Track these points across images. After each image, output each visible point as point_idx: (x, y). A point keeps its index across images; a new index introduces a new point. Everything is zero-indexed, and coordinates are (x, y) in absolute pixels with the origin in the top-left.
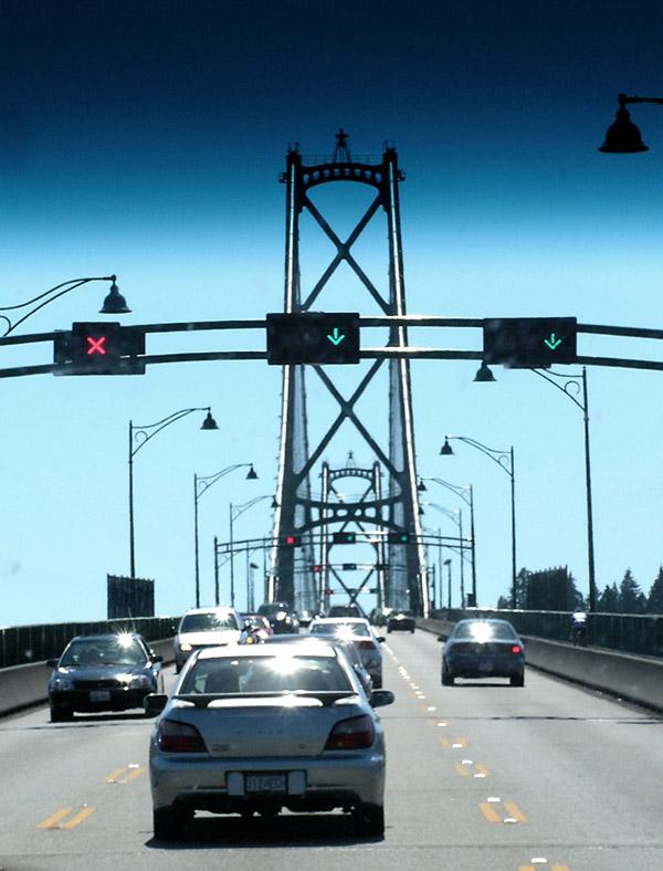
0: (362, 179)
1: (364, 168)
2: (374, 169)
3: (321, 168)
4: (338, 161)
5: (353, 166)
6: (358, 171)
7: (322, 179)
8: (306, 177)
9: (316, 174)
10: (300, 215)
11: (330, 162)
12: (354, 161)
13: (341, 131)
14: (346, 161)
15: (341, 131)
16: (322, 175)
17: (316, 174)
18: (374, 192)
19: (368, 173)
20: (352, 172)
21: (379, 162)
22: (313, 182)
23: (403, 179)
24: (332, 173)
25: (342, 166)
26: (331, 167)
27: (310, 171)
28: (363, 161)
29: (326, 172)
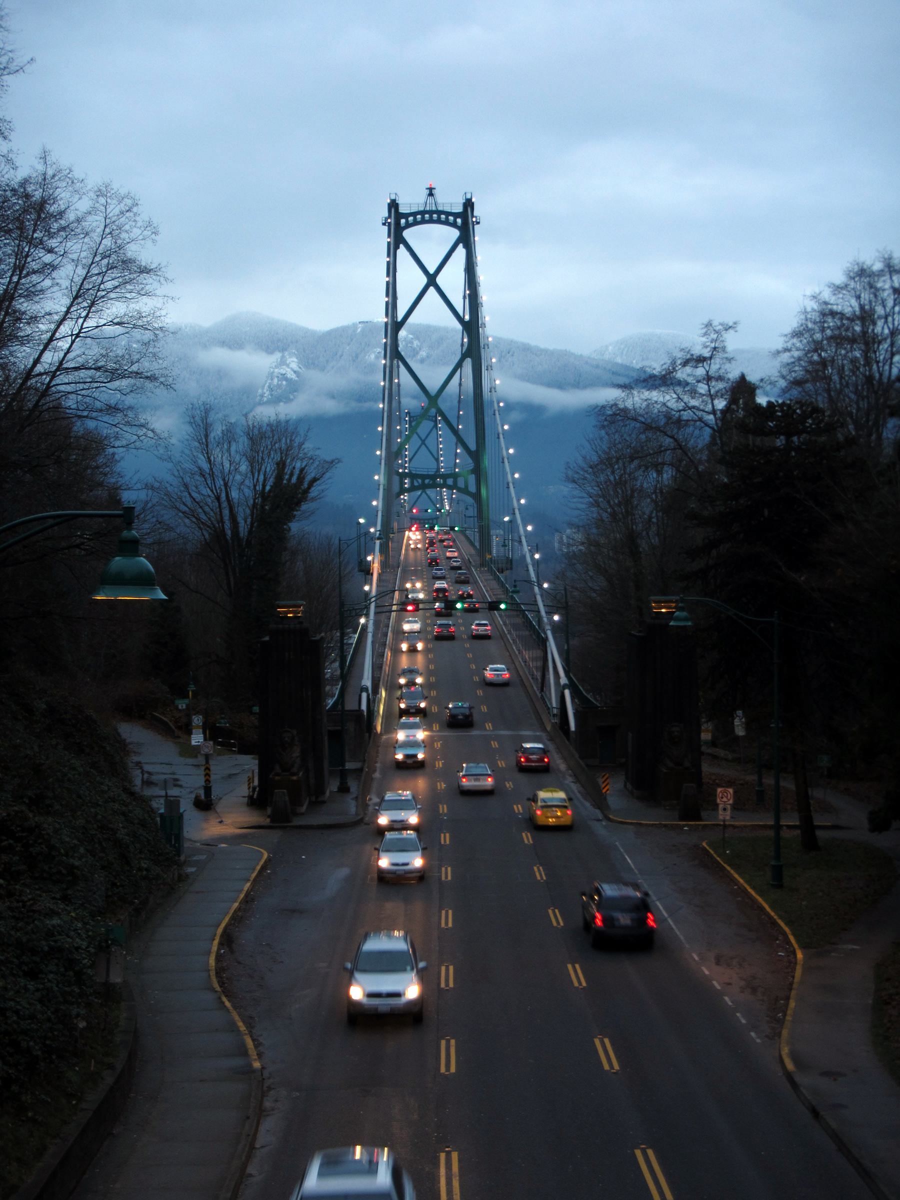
0: (446, 223)
1: (448, 214)
2: (456, 215)
3: (414, 214)
4: (428, 209)
5: (440, 213)
6: (443, 216)
7: (416, 223)
8: (403, 221)
9: (411, 219)
10: (398, 251)
11: (422, 209)
12: (440, 208)
13: (431, 185)
14: (434, 209)
15: (431, 185)
16: (415, 219)
17: (411, 219)
18: (455, 233)
19: (451, 218)
20: (439, 217)
21: (459, 209)
22: (408, 225)
23: (478, 223)
24: (423, 217)
25: (431, 213)
26: (422, 213)
27: (406, 216)
28: (447, 209)
29: (419, 217)
